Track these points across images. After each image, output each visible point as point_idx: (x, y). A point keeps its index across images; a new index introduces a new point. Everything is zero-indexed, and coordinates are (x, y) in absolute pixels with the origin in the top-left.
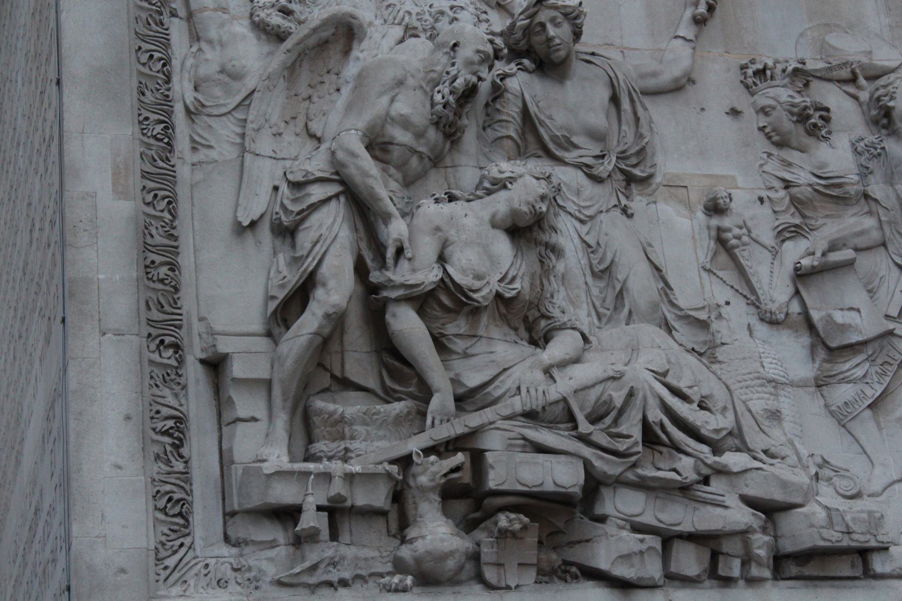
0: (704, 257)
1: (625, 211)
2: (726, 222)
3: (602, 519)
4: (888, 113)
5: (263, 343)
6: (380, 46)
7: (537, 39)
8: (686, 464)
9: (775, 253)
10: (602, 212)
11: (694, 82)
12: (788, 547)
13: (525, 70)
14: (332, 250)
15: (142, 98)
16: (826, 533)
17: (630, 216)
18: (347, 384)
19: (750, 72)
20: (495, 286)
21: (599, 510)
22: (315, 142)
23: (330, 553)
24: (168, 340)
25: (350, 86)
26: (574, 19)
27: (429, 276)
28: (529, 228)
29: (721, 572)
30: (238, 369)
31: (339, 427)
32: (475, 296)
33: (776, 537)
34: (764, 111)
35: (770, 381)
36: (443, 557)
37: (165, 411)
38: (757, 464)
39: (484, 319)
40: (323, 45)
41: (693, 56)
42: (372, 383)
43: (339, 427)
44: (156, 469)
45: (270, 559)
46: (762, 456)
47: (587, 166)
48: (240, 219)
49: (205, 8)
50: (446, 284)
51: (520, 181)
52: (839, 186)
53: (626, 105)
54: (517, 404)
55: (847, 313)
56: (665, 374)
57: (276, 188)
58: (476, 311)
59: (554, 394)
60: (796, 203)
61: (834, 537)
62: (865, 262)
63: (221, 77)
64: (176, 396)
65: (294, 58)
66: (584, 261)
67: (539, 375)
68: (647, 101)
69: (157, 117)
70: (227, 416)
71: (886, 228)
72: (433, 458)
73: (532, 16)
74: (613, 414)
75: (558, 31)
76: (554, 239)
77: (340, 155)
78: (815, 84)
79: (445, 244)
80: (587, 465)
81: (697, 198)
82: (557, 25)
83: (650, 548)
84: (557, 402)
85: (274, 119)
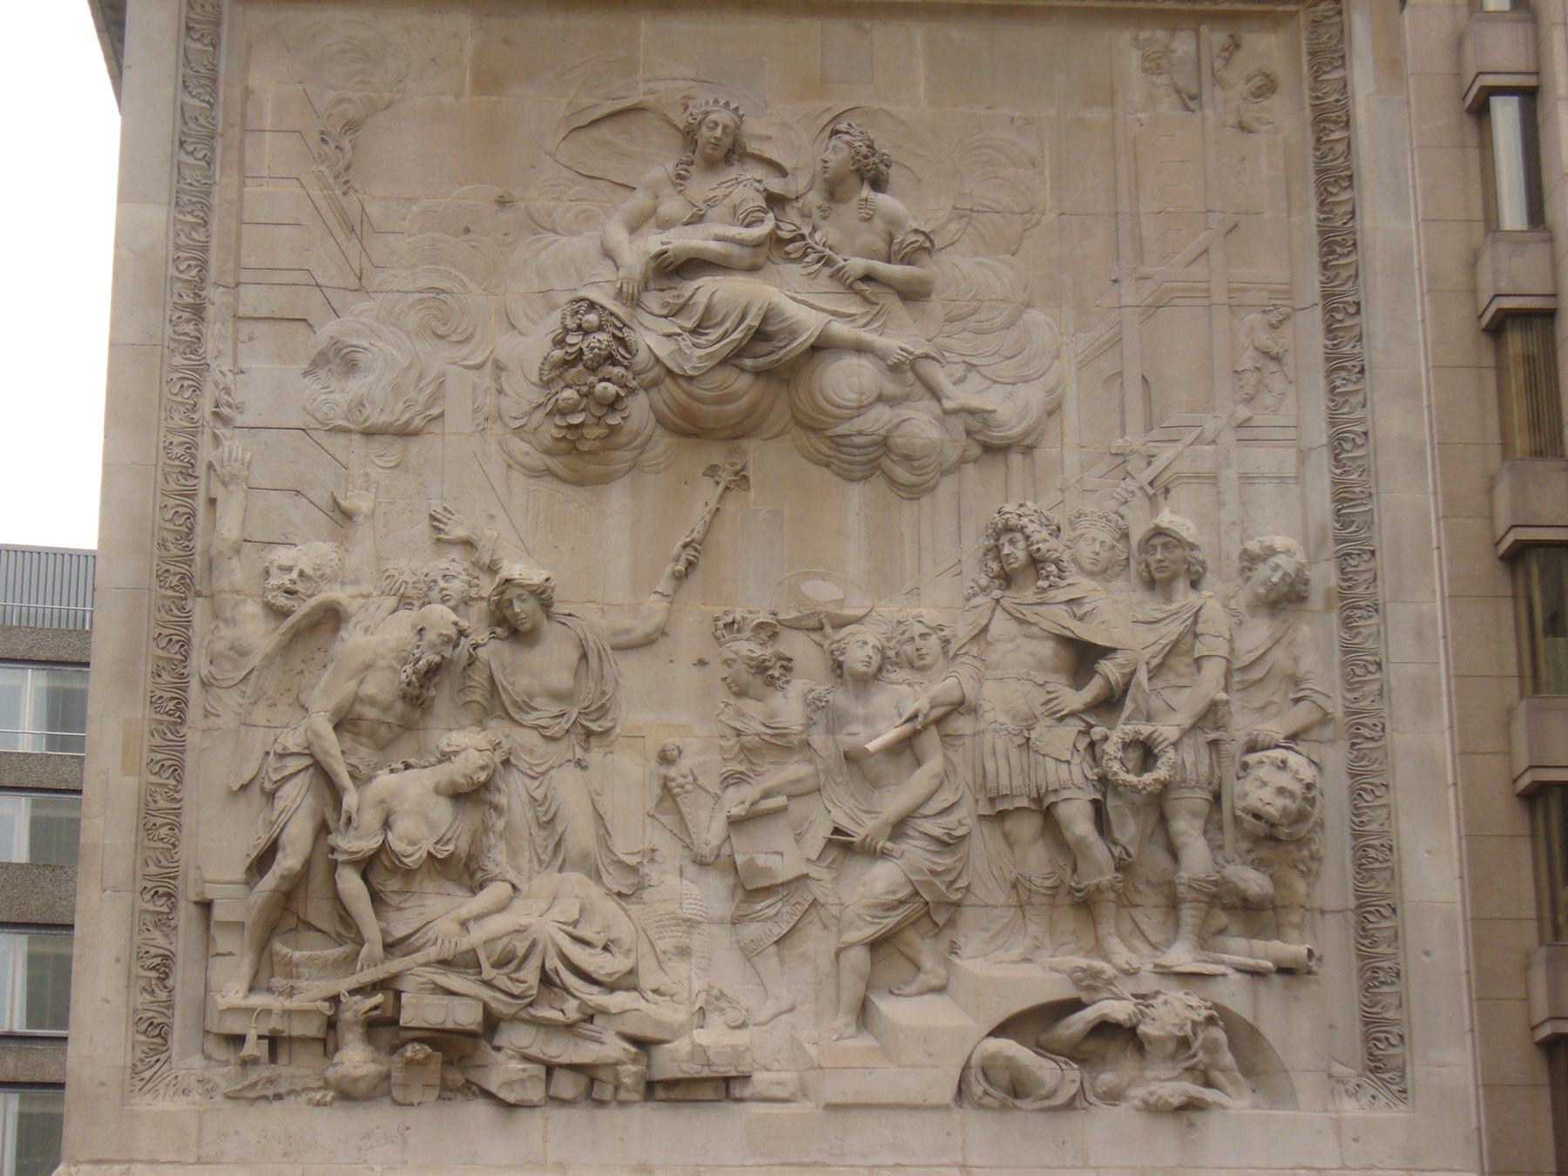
0: (651, 805)
1: (579, 763)
2: (672, 772)
3: (498, 1049)
4: (840, 665)
5: (240, 889)
7: (508, 612)
8: (571, 1005)
9: (717, 798)
12: (658, 1075)
15: (158, 680)
16: (685, 1067)
17: (585, 768)
18: (309, 926)
19: (720, 624)
21: (498, 1041)
23: (266, 1073)
24: (161, 890)
27: (369, 844)
28: (477, 791)
29: (595, 1095)
30: (218, 914)
31: (291, 969)
33: (648, 1066)
34: (727, 662)
35: (684, 921)
36: (356, 1080)
37: (153, 951)
38: (642, 1004)
39: (419, 878)
41: (669, 611)
42: (325, 926)
43: (291, 969)
44: (140, 999)
45: (223, 1076)
46: (650, 995)
51: (463, 755)
52: (784, 736)
54: (432, 953)
55: (771, 857)
56: (575, 924)
58: (409, 873)
59: (465, 943)
60: (747, 752)
61: (693, 1070)
62: (797, 808)
64: (166, 936)
66: (530, 814)
67: (455, 928)
68: (619, 657)
70: (212, 952)
71: (823, 778)
72: (357, 998)
74: (516, 961)
78: (785, 634)
80: (487, 1010)
82: (524, 601)
83: (531, 1077)
84: (468, 952)
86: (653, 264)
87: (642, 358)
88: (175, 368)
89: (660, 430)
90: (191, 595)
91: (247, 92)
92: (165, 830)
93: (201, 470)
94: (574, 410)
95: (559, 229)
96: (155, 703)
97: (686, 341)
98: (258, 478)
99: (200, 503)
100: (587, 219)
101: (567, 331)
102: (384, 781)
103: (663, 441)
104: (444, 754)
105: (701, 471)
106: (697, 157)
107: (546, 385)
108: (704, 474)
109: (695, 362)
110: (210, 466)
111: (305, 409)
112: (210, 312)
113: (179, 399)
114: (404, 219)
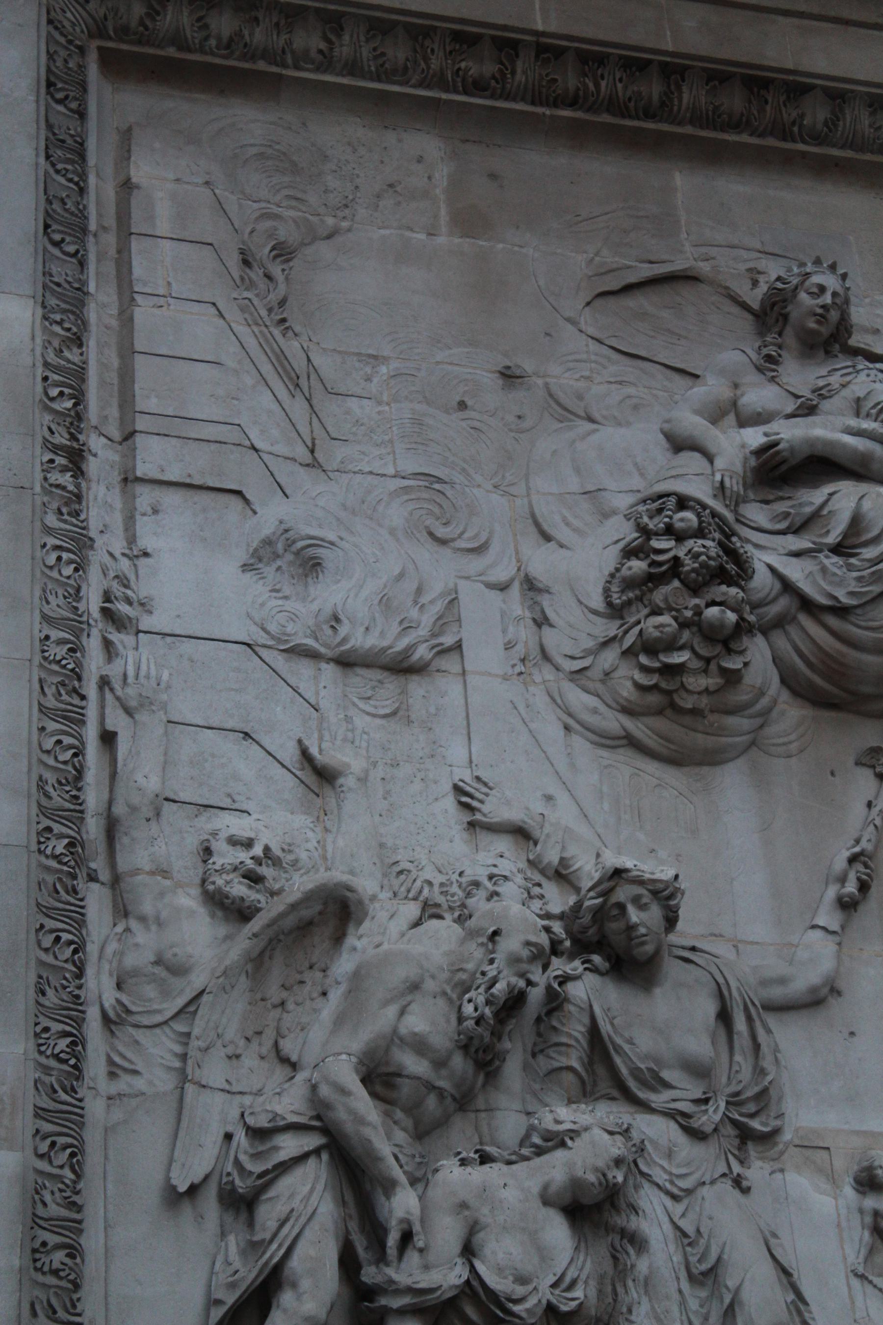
0: (854, 1254)
1: (737, 1182)
6: (386, 933)
7: (614, 926)
10: (704, 1183)
11: (839, 993)
13: (595, 970)
14: (307, 1233)
15: (42, 1000)
17: (746, 1191)
20: (545, 1294)
22: (288, 1070)
25: (343, 988)
26: (666, 897)
28: (598, 1207)
32: (516, 1308)
40: (305, 928)
41: (839, 956)
47: (684, 1115)
48: (174, 1182)
49: (137, 871)
50: (473, 1289)
51: (585, 1136)
53: (740, 1024)
57: (228, 1137)
63: (158, 970)
65: (262, 944)
66: (677, 1258)
68: (771, 1020)
69: (61, 1027)
73: (606, 894)
75: (644, 915)
76: (634, 1223)
77: (325, 1091)
79: (473, 1229)
81: (844, 1166)
82: (642, 907)
85: (231, 1032)
86: (753, 462)
87: (761, 581)
88: (48, 530)
89: (785, 695)
90: (82, 875)
91: (127, 186)
92: (59, 1257)
93: (91, 690)
94: (671, 646)
95: (597, 416)
96: (40, 1034)
97: (832, 562)
98: (185, 707)
99: (91, 733)
100: (636, 407)
101: (646, 533)
102: (453, 1177)
103: (791, 714)
104: (549, 1136)
105: (851, 761)
106: (790, 338)
107: (615, 611)
108: (858, 763)
109: (853, 587)
110: (104, 683)
111: (248, 615)
112: (92, 466)
113: (55, 574)
114: (368, 379)
